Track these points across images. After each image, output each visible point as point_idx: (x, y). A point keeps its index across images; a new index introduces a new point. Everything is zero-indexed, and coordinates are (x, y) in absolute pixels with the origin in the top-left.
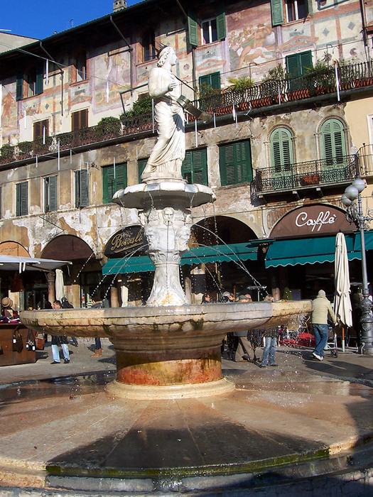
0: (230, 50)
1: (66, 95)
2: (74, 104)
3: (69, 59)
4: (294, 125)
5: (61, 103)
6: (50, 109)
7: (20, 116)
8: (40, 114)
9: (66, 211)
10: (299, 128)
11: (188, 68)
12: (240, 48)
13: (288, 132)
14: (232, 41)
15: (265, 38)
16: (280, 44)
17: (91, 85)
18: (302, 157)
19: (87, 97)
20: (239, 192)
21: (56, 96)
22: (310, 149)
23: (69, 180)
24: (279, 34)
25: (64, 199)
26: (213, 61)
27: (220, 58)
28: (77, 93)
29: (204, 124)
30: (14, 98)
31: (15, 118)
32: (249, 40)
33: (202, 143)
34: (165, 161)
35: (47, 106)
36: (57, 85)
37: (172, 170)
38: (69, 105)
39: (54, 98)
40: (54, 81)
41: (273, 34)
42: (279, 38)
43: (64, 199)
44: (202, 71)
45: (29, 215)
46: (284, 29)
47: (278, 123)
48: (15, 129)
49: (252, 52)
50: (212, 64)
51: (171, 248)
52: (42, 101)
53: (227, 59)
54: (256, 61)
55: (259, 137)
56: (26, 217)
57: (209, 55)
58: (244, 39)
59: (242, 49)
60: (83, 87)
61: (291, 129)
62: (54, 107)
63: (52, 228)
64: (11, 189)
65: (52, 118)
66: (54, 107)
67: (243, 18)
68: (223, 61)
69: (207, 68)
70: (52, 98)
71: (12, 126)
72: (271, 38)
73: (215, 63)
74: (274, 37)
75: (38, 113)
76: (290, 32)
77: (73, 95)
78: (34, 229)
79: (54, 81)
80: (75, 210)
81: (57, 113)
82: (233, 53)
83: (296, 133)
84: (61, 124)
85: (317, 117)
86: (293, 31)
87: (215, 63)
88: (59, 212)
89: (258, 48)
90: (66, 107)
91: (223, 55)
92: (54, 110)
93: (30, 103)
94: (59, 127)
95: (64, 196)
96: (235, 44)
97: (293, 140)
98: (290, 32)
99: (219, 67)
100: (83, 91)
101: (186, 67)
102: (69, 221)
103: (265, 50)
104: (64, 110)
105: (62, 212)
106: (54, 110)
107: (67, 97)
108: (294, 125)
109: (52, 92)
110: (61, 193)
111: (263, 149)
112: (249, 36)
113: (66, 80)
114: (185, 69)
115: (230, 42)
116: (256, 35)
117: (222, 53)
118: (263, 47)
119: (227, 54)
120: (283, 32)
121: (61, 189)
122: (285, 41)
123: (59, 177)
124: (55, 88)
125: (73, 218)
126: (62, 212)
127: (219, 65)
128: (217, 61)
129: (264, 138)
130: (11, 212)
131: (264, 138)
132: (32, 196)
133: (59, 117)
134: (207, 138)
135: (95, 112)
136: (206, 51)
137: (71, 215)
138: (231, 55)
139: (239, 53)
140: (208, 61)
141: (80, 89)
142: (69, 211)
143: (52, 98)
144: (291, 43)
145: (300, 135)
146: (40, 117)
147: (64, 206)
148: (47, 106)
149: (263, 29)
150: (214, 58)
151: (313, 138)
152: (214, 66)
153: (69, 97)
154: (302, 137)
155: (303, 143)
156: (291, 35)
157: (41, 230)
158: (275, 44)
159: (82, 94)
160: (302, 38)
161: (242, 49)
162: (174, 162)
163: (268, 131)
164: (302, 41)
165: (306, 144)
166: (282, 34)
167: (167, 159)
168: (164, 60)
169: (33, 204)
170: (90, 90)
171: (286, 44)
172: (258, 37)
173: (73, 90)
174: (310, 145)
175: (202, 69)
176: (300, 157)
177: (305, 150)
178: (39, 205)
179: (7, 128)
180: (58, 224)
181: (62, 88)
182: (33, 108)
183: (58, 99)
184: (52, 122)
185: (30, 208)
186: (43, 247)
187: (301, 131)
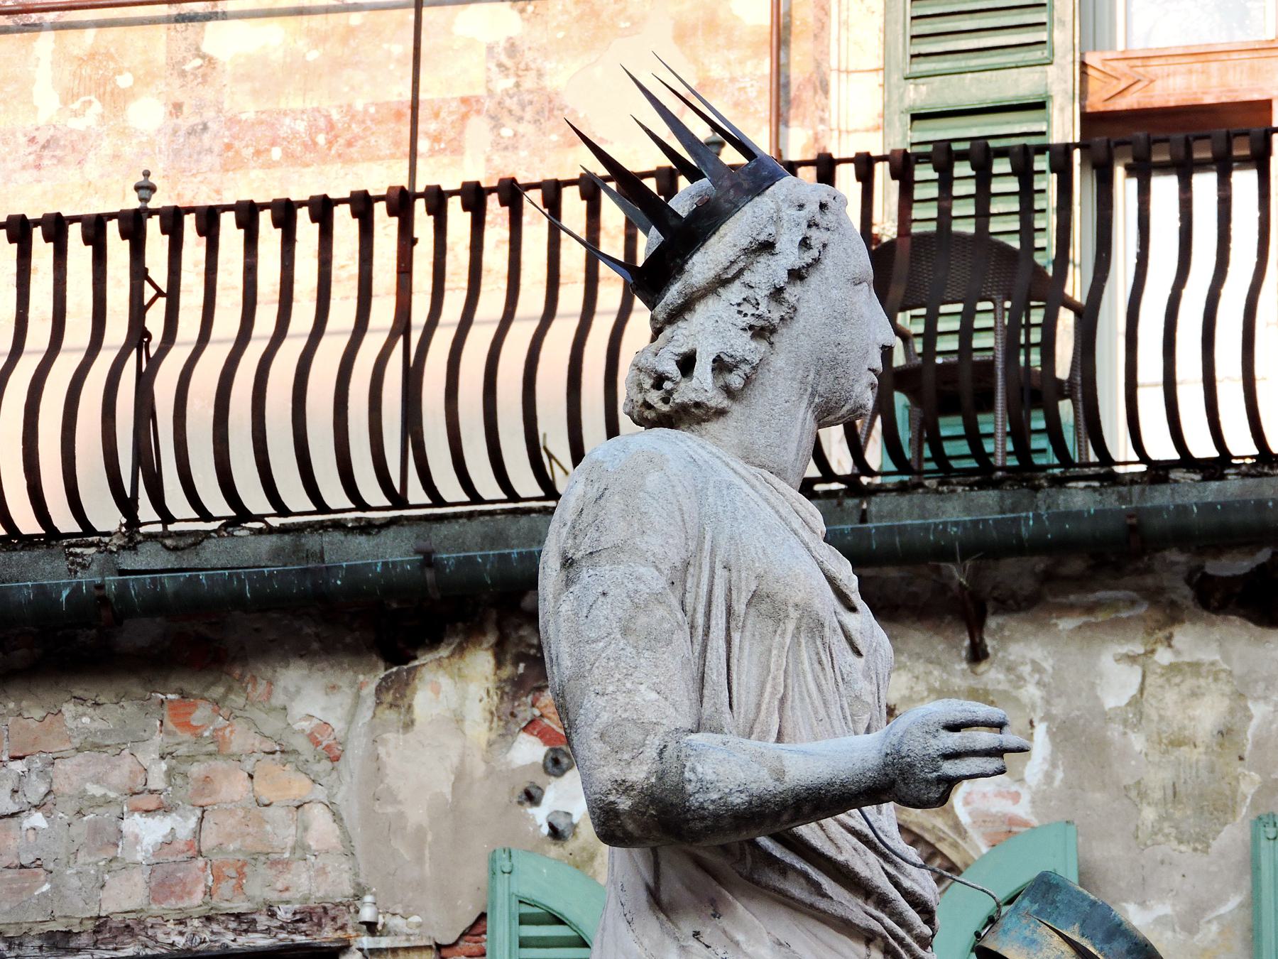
168: (744, 346)
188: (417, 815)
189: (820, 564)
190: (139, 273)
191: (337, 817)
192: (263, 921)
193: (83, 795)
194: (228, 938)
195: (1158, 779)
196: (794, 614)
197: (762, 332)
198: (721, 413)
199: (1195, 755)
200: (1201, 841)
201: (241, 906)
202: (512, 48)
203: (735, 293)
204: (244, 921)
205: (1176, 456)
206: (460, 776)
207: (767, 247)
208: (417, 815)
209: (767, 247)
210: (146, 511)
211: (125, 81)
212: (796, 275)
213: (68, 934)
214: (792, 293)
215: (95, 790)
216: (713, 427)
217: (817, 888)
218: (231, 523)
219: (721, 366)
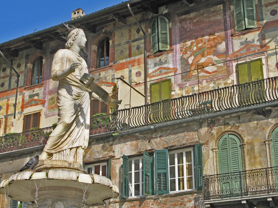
0: (182, 58)
1: (20, 98)
2: (26, 107)
3: (26, 63)
4: (243, 131)
5: (15, 105)
10: (249, 135)
11: (140, 75)
12: (191, 56)
13: (237, 139)
14: (184, 50)
15: (215, 46)
16: (230, 52)
17: (45, 89)
18: (251, 164)
19: (40, 100)
20: (186, 200)
21: (10, 99)
22: (260, 156)
24: (230, 43)
26: (165, 68)
27: (171, 66)
28: (31, 96)
29: (151, 129)
32: (199, 49)
33: (149, 148)
34: (64, 148)
37: (71, 159)
38: (23, 108)
39: (8, 100)
40: (10, 84)
41: (224, 44)
42: (230, 46)
44: (153, 79)
46: (234, 38)
47: (226, 129)
49: (203, 60)
50: (164, 71)
53: (179, 67)
54: (208, 69)
55: (207, 143)
57: (161, 63)
58: (195, 48)
59: (193, 57)
60: (37, 90)
61: (240, 135)
62: (7, 109)
65: (4, 120)
66: (7, 109)
67: (194, 28)
68: (174, 68)
69: (159, 75)
70: (6, 100)
72: (222, 47)
73: (166, 71)
74: (225, 46)
76: (240, 41)
77: (27, 98)
79: (10, 84)
81: (10, 115)
82: (184, 61)
83: (246, 139)
84: (13, 126)
85: (267, 124)
86: (243, 40)
87: (166, 71)
89: (208, 57)
90: (18, 110)
91: (174, 62)
92: (7, 112)
94: (10, 129)
96: (186, 53)
97: (242, 146)
98: (240, 41)
99: (170, 74)
100: (37, 95)
101: (138, 74)
103: (215, 58)
104: (17, 112)
106: (7, 112)
107: (21, 100)
108: (243, 131)
111: (211, 156)
112: (200, 45)
114: (137, 76)
115: (181, 51)
116: (207, 45)
117: (173, 61)
118: (214, 55)
119: (179, 62)
120: (233, 41)
122: (236, 50)
127: (170, 72)
128: (169, 69)
129: (212, 144)
131: (212, 144)
134: (154, 144)
135: (47, 116)
136: (158, 59)
138: (182, 63)
139: (190, 61)
140: (160, 68)
141: (34, 93)
143: (6, 100)
144: (242, 52)
145: (249, 141)
149: (214, 39)
150: (165, 66)
151: (262, 145)
152: (166, 73)
153: (23, 100)
154: (251, 144)
155: (253, 149)
156: (242, 44)
158: (225, 52)
159: (36, 98)
160: (253, 46)
161: (193, 57)
162: (75, 150)
163: (216, 137)
164: (252, 49)
165: (256, 151)
166: (232, 42)
167: (66, 146)
168: (72, 42)
170: (44, 94)
171: (237, 52)
172: (208, 46)
173: (27, 93)
174: (260, 152)
175: (154, 76)
176: (249, 165)
177: (255, 158)
183: (12, 101)
184: (4, 123)
187: (249, 138)
188: (203, 134)
189: (76, 58)
190: (182, 101)
191: (198, 136)
192: (193, 143)
193: (181, 136)
194: (191, 144)
195: (252, 126)
196: (71, 61)
197: (73, 40)
198: (70, 47)
199: (255, 124)
200: (256, 130)
201: (192, 142)
202: (213, 87)
203: (71, 37)
204: (192, 143)
205: (251, 104)
206: (205, 132)
207: (74, 33)
208: (203, 134)
209: (74, 33)
210: (183, 117)
211: (189, 92)
212: (76, 36)
213: (181, 145)
215: (182, 135)
216: (70, 49)
217: (71, 82)
218: (189, 117)
219: (70, 44)
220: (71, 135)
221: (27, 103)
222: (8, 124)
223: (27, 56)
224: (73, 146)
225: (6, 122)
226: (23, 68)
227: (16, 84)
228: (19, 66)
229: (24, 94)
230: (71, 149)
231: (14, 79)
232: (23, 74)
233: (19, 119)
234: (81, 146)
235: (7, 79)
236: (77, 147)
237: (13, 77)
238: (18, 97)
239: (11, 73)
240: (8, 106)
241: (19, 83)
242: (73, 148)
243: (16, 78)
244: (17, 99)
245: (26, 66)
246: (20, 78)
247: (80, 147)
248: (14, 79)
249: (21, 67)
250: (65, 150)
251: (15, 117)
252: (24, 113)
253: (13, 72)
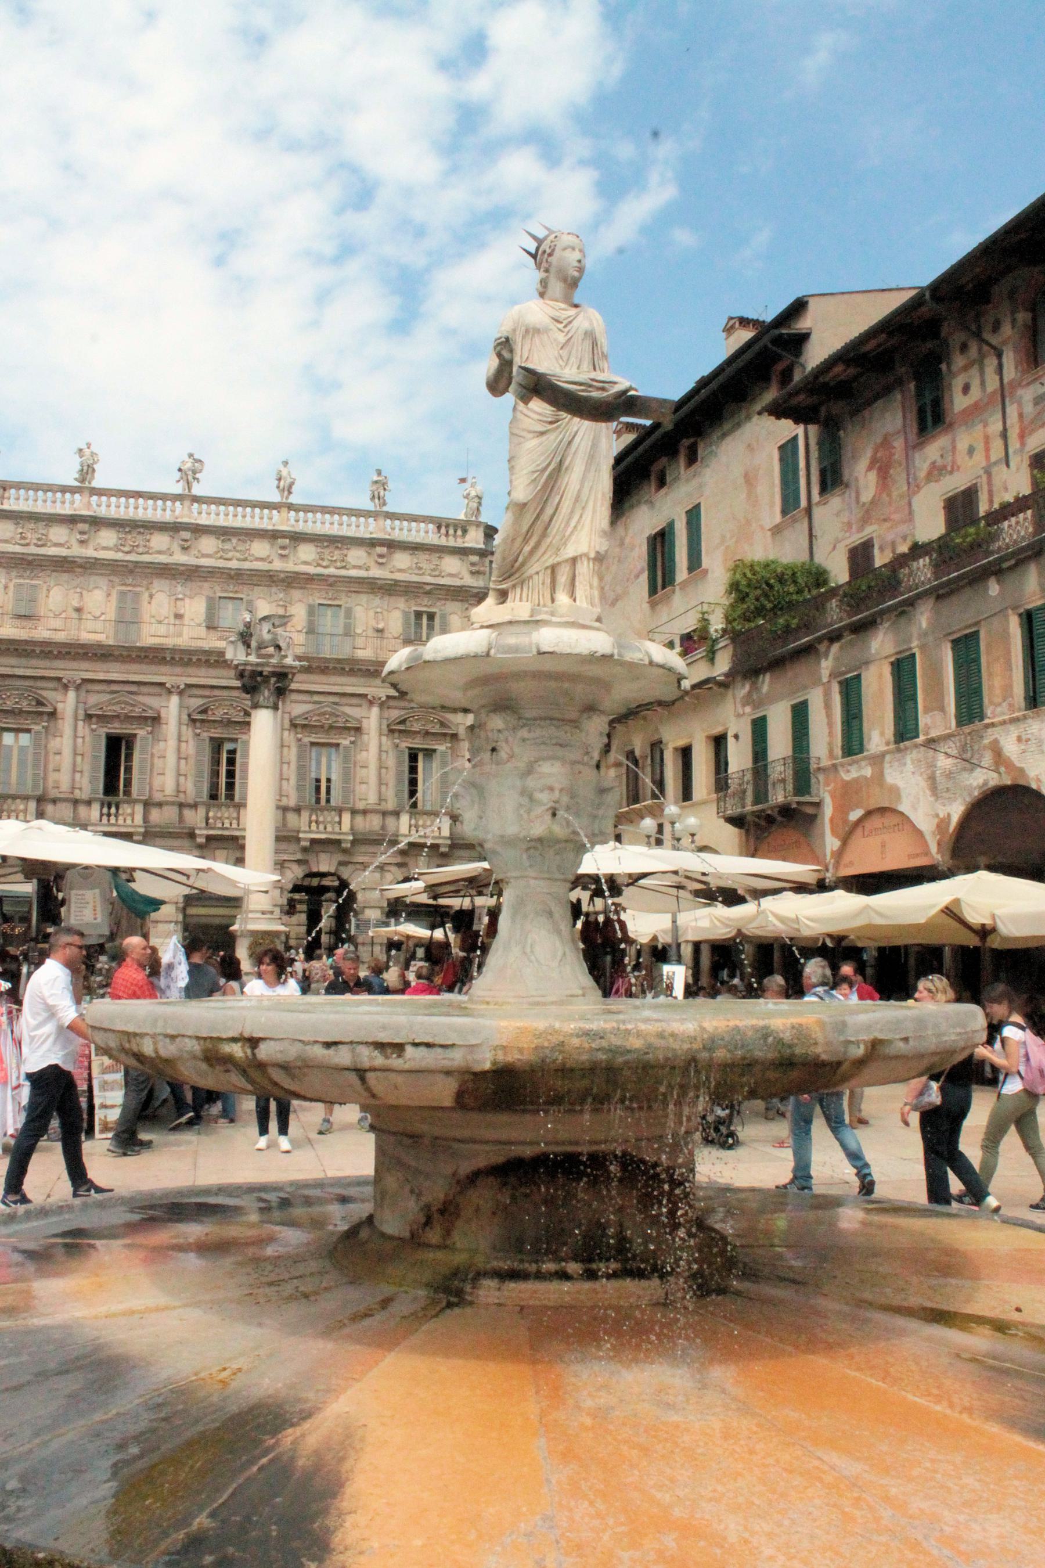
1: (1012, 411)
2: (1033, 431)
5: (1004, 435)
6: (979, 457)
7: (914, 487)
8: (956, 474)
9: (1004, 723)
23: (1006, 636)
25: (998, 692)
30: (898, 444)
31: (901, 496)
35: (971, 451)
36: (990, 389)
38: (1022, 437)
39: (986, 425)
40: (983, 383)
43: (998, 692)
45: (922, 738)
48: (904, 522)
51: (512, 830)
52: (958, 439)
56: (916, 746)
62: (987, 450)
63: (972, 770)
64: (880, 676)
65: (984, 478)
66: (987, 450)
71: (896, 517)
75: (951, 472)
77: (1029, 409)
78: (934, 773)
79: (983, 383)
80: (1025, 717)
81: (995, 463)
88: (987, 726)
90: (1014, 444)
92: (988, 457)
93: (933, 450)
95: (998, 682)
102: (1010, 747)
104: (1011, 451)
105: (993, 725)
106: (988, 457)
109: (975, 411)
110: (990, 675)
113: (1010, 372)
121: (988, 663)
123: (982, 635)
124: (986, 400)
125: (1019, 739)
126: (993, 725)
130: (882, 734)
132: (925, 691)
133: (1001, 474)
137: (1014, 731)
142: (1014, 721)
143: (980, 427)
146: (955, 483)
147: (999, 709)
148: (971, 451)
153: (1021, 416)
157: (949, 775)
169: (927, 710)
178: (942, 709)
179: (887, 525)
180: (987, 759)
181: (1003, 394)
182: (940, 462)
183: (996, 427)
184: (985, 488)
185: (923, 720)
186: (955, 819)
209: (544, 252)
214: (550, 259)
220: (549, 530)
221: (1032, 422)
222: (995, 489)
223: (1012, 295)
224: (558, 559)
225: (990, 483)
226: (1007, 330)
227: (997, 378)
228: (996, 327)
229: (1021, 397)
230: (553, 569)
231: (991, 363)
232: (1010, 346)
233: (1018, 469)
234: (586, 555)
235: (974, 371)
236: (574, 560)
237: (987, 361)
238: (1008, 410)
239: (980, 350)
240: (987, 440)
241: (1005, 371)
242: (559, 564)
243: (995, 362)
244: (1007, 415)
245: (1014, 321)
246: (1005, 360)
247: (581, 556)
248: (991, 363)
249: (1002, 329)
250: (537, 573)
251: (1008, 465)
252: (1028, 448)
253: (985, 348)
